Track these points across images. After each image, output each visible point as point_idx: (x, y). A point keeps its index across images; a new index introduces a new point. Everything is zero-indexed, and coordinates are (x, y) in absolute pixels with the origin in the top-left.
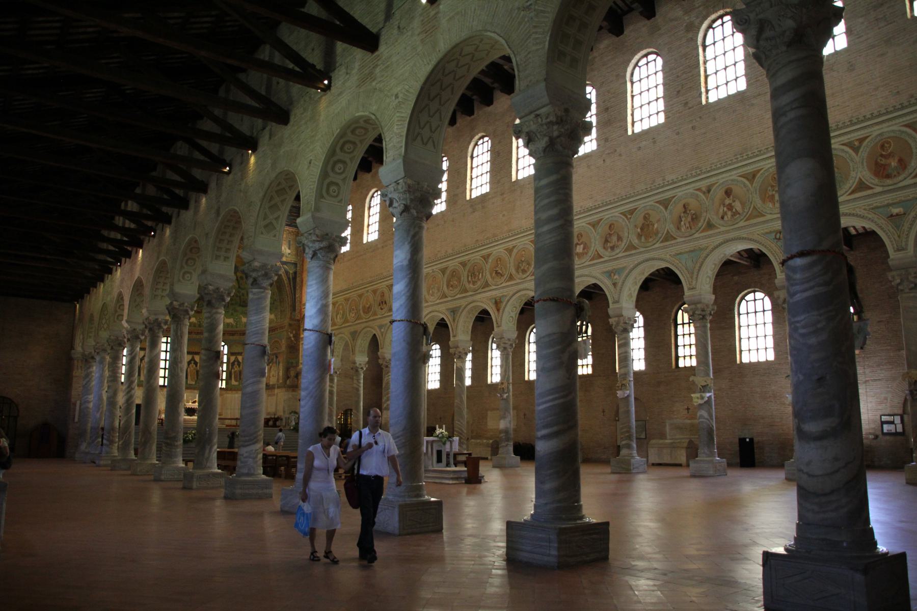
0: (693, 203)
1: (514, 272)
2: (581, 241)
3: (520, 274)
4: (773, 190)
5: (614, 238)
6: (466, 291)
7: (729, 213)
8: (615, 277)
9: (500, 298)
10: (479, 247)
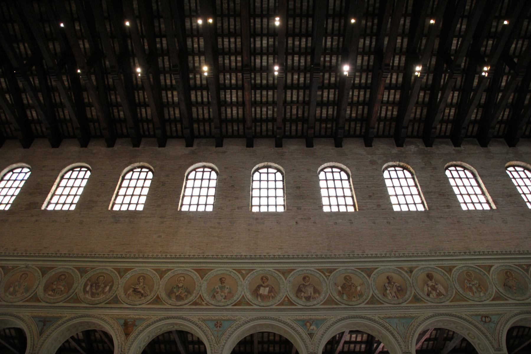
0: (396, 277)
1: (163, 295)
3: (174, 300)
4: (470, 284)
6: (77, 300)
8: (312, 328)
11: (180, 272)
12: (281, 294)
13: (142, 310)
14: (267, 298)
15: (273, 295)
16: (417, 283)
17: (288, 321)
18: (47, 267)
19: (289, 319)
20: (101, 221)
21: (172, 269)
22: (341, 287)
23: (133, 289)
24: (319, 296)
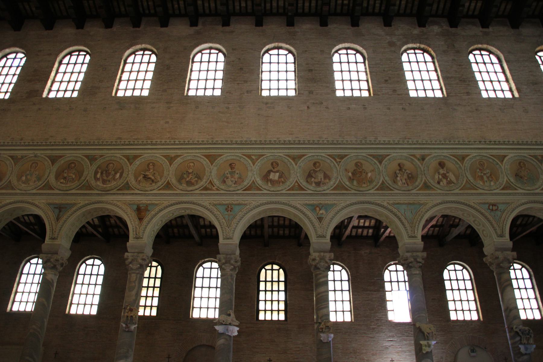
0: (407, 164)
1: (174, 181)
3: (185, 185)
4: (481, 173)
5: (320, 176)
6: (89, 187)
8: (321, 212)
9: (147, 205)
10: (123, 145)
11: (189, 158)
12: (291, 179)
13: (153, 196)
14: (277, 183)
15: (283, 180)
16: (428, 171)
17: (298, 205)
18: (56, 156)
19: (299, 203)
20: (105, 108)
21: (181, 155)
22: (352, 173)
23: (143, 175)
24: (329, 181)
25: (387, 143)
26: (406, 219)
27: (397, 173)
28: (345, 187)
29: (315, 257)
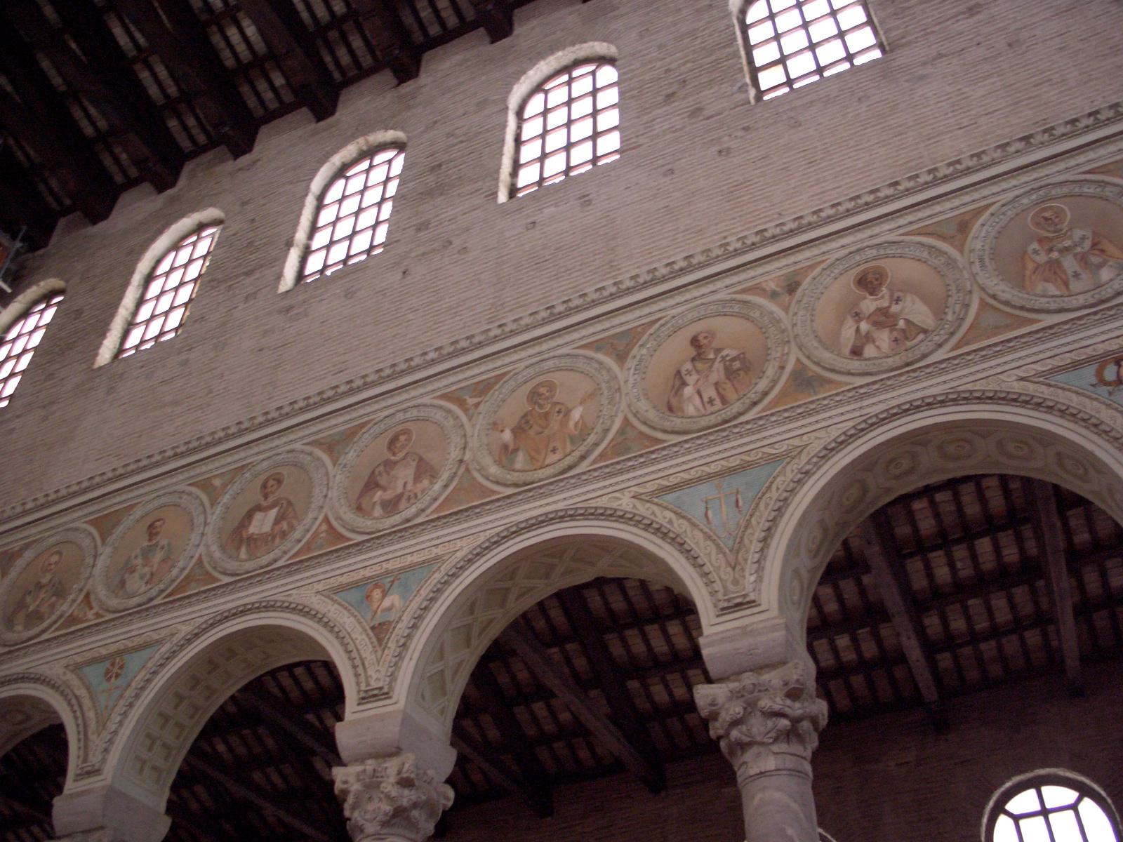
2: (271, 499)
4: (1051, 250)
7: (884, 338)
8: (387, 602)
22: (514, 431)
25: (645, 283)
26: (709, 538)
27: (683, 372)
28: (482, 486)
29: (346, 782)
